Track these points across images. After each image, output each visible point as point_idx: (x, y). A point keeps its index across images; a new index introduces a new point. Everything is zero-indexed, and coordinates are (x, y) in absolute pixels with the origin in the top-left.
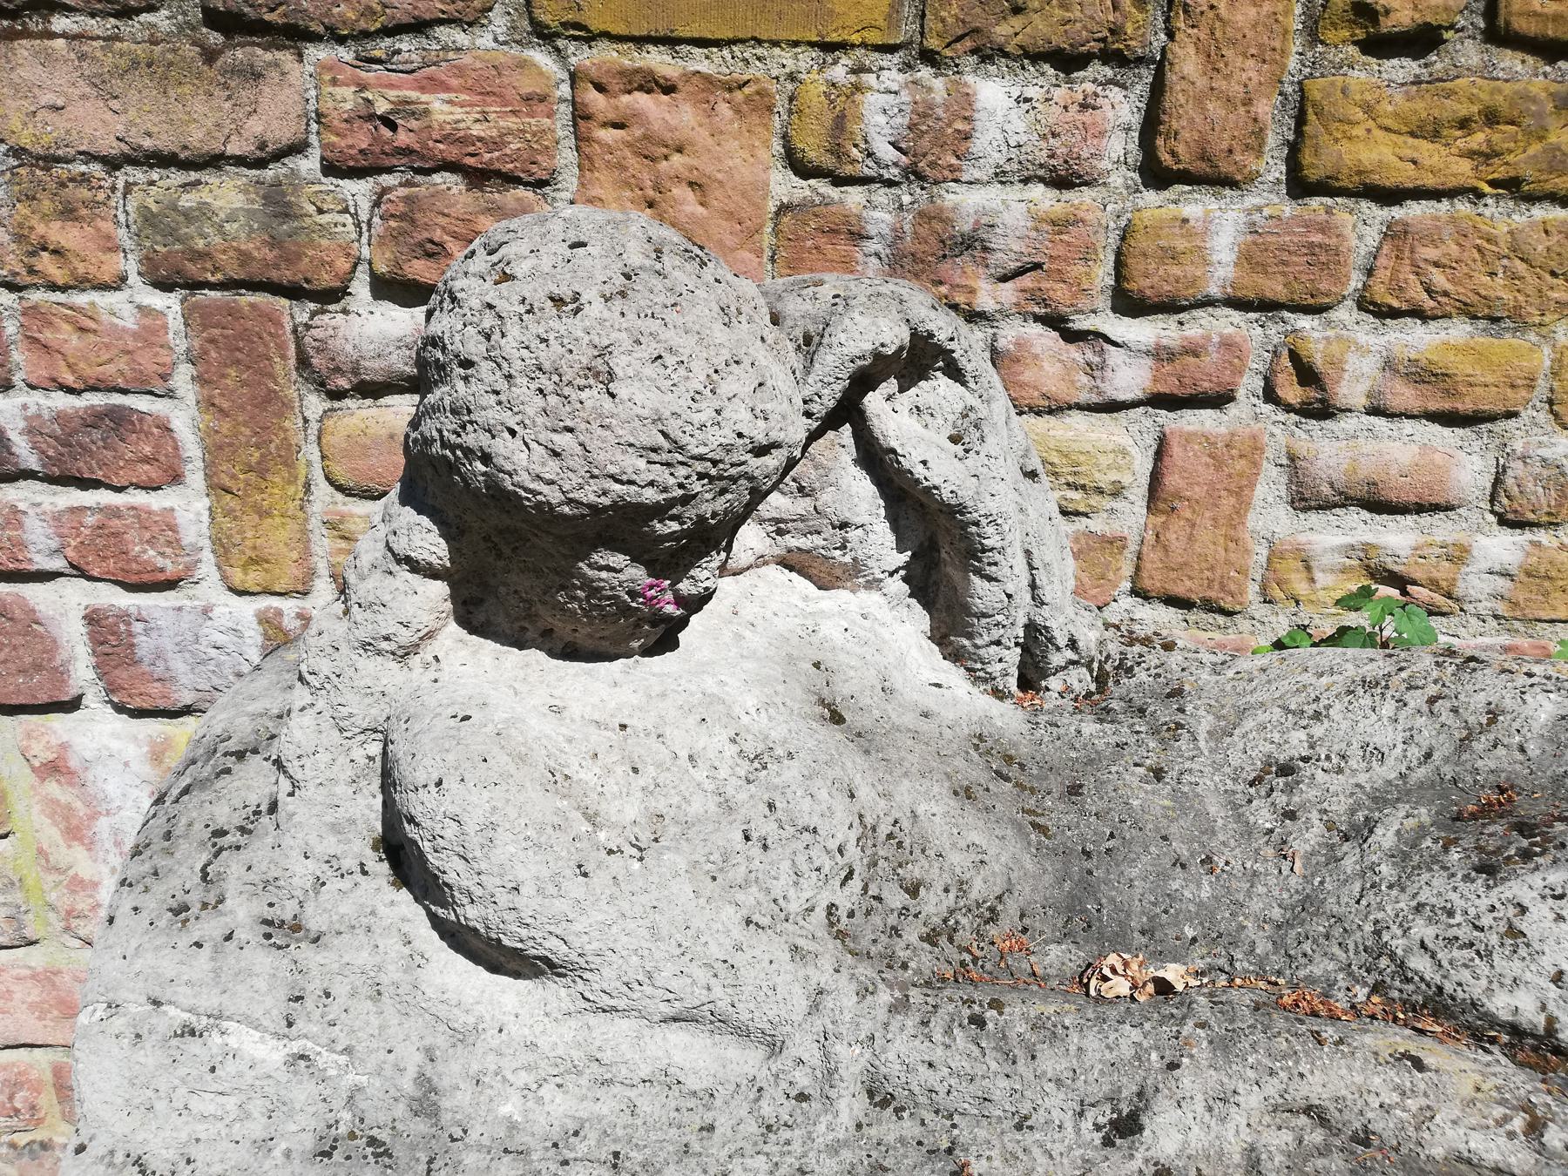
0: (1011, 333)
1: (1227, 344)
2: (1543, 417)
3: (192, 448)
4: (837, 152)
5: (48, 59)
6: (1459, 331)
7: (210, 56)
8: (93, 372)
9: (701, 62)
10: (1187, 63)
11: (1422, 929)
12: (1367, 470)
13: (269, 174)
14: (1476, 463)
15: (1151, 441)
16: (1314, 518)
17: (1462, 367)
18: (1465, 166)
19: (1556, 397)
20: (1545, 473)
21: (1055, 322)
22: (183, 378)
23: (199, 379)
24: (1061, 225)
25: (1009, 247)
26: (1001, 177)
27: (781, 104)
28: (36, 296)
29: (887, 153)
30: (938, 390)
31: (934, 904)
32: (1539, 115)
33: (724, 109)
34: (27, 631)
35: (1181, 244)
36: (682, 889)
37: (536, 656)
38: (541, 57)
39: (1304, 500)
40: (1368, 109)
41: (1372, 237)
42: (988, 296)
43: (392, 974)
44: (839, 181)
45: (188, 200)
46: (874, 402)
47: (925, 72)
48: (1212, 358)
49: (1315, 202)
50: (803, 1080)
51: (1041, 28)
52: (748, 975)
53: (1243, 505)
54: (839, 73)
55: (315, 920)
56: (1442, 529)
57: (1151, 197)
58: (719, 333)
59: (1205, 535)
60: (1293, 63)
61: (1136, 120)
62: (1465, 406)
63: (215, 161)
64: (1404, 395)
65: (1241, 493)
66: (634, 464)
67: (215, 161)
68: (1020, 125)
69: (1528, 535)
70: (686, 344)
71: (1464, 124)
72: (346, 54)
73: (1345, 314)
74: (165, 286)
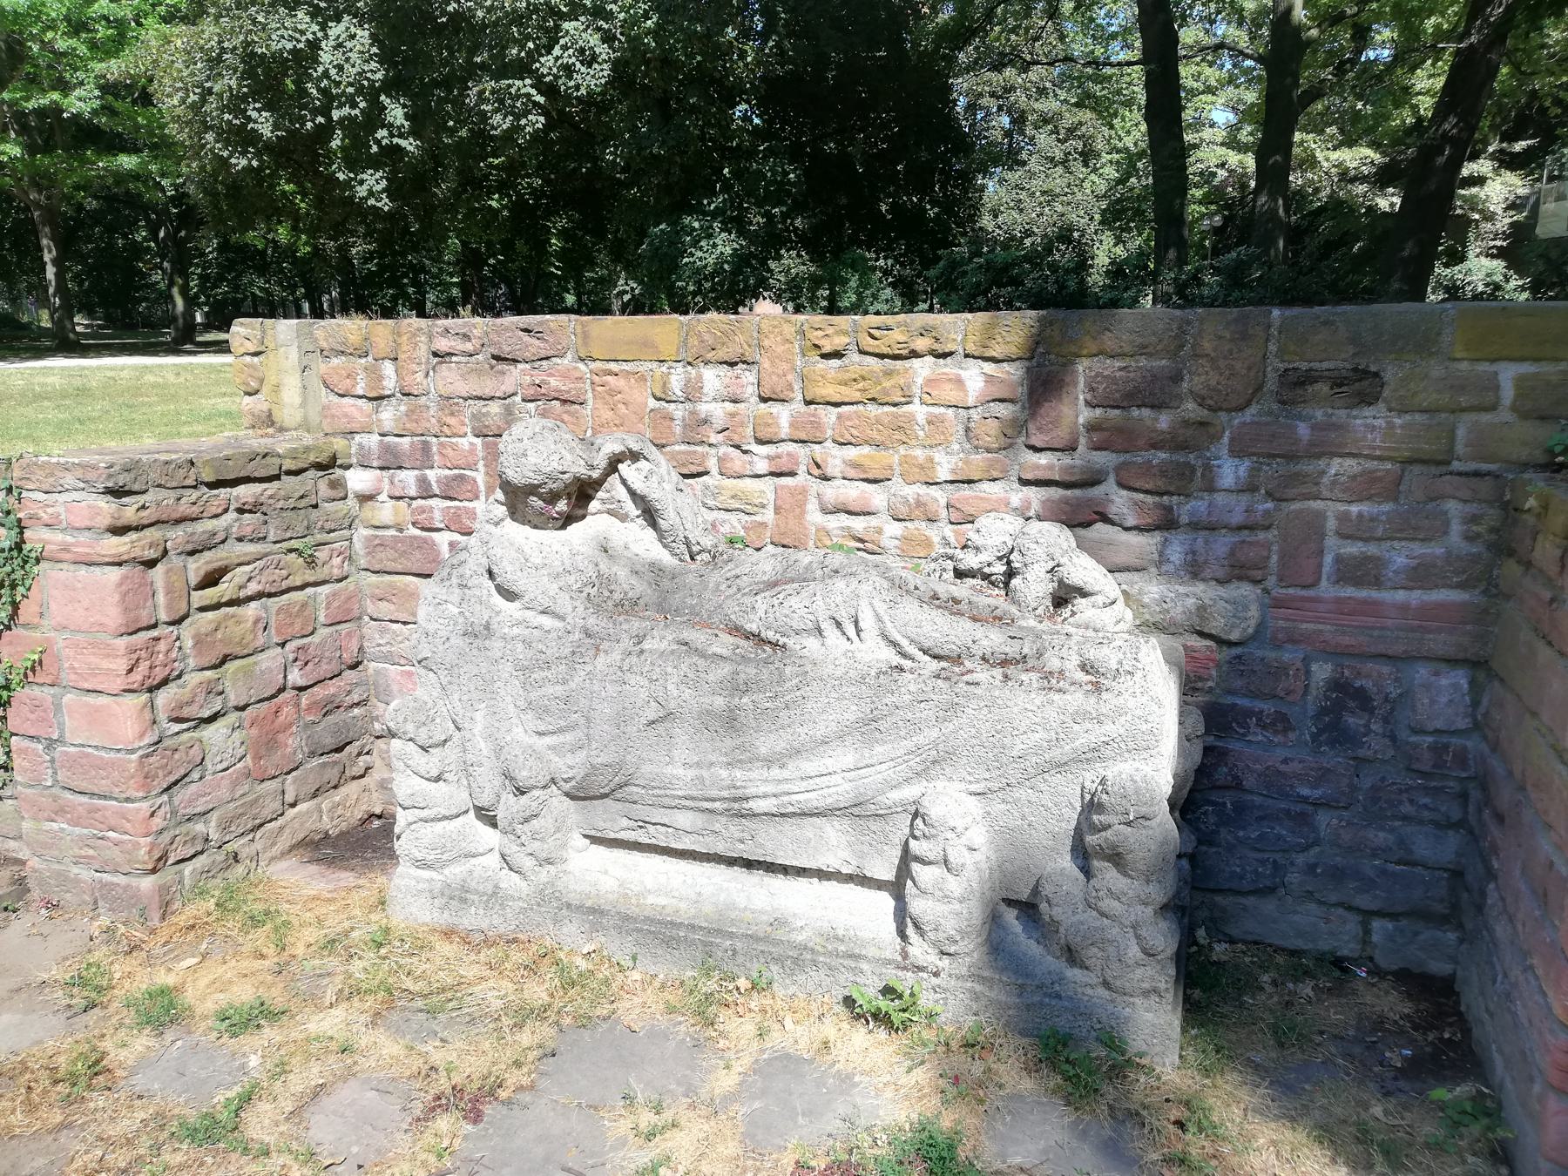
0: (723, 450)
1: (789, 454)
2: (900, 480)
3: (482, 488)
4: (664, 392)
5: (450, 369)
6: (866, 450)
7: (492, 367)
8: (455, 463)
9: (625, 366)
10: (766, 364)
11: (737, 609)
12: (841, 499)
13: (507, 401)
14: (882, 497)
15: (772, 488)
16: (829, 516)
17: (867, 462)
18: (858, 394)
21: (737, 447)
22: (481, 465)
23: (485, 465)
24: (733, 415)
25: (719, 423)
26: (714, 399)
27: (649, 379)
28: (442, 439)
29: (680, 394)
30: (642, 464)
31: (617, 596)
32: (877, 377)
33: (633, 380)
34: (432, 549)
35: (770, 421)
36: (545, 579)
37: (527, 527)
38: (581, 366)
39: (826, 511)
40: (823, 377)
41: (834, 418)
42: (714, 438)
43: (484, 598)
44: (668, 402)
45: (484, 410)
46: (620, 466)
47: (690, 368)
48: (785, 459)
49: (813, 407)
50: (569, 628)
51: (722, 354)
52: (559, 601)
53: (803, 512)
54: (664, 369)
55: (470, 585)
56: (873, 521)
57: (763, 405)
58: (553, 446)
59: (791, 523)
60: (799, 363)
61: (756, 381)
62: (870, 476)
63: (492, 398)
64: (852, 473)
65: (802, 505)
66: (532, 474)
67: (492, 398)
68: (717, 384)
69: (904, 524)
70: (543, 449)
71: (855, 380)
72: (528, 366)
73: (829, 444)
74: (478, 436)
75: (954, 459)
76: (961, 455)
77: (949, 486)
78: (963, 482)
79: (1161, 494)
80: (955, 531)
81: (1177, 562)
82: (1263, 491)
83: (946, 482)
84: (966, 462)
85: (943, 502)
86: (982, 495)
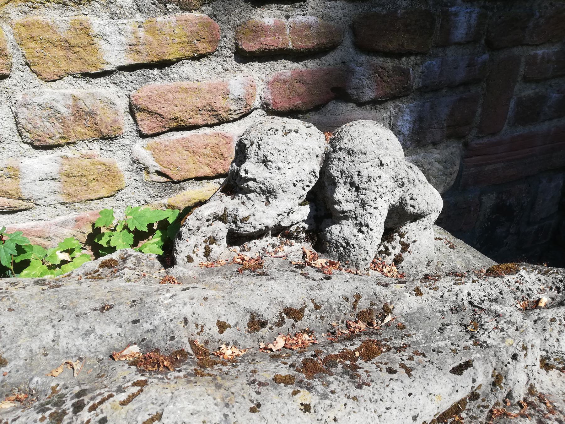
2: (28, 75)
19: (30, 60)
20: (45, 113)
69: (57, 153)
75: (129, 25)
76: (139, 17)
77: (127, 77)
78: (151, 66)
79: (397, 55)
80: (153, 149)
81: (407, 133)
82: (483, 41)
83: (122, 69)
84: (153, 30)
85: (122, 104)
86: (185, 83)
